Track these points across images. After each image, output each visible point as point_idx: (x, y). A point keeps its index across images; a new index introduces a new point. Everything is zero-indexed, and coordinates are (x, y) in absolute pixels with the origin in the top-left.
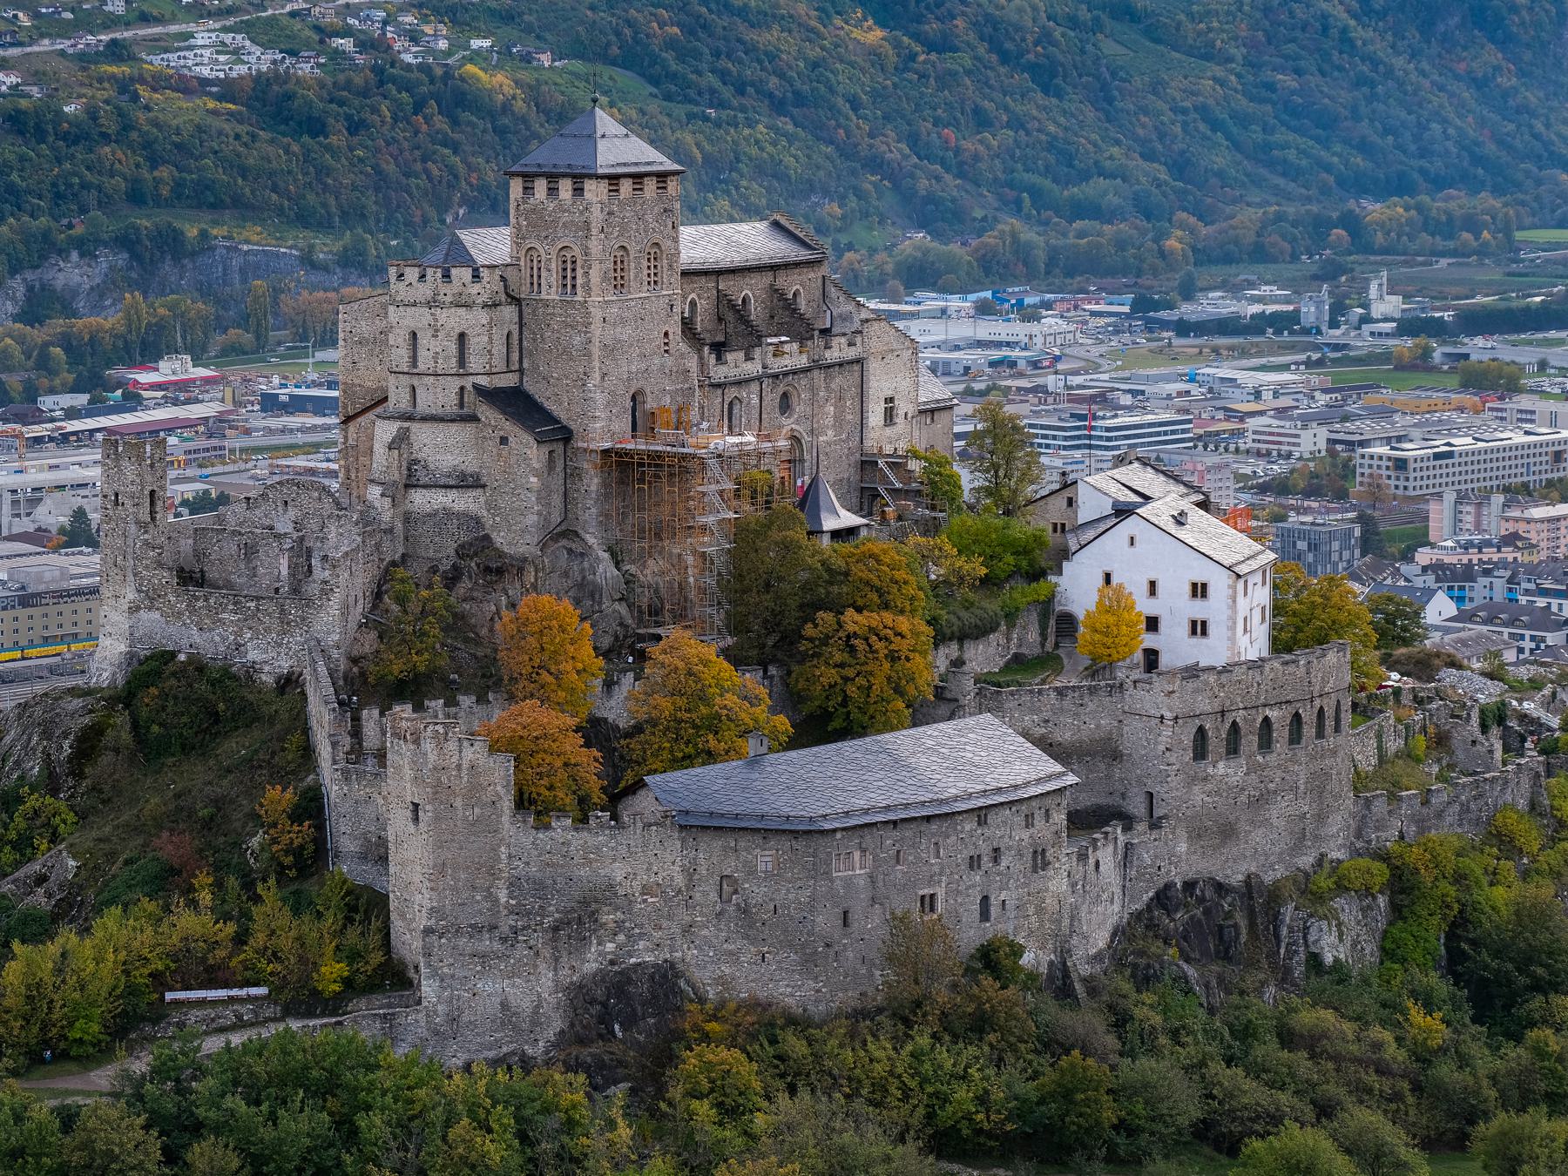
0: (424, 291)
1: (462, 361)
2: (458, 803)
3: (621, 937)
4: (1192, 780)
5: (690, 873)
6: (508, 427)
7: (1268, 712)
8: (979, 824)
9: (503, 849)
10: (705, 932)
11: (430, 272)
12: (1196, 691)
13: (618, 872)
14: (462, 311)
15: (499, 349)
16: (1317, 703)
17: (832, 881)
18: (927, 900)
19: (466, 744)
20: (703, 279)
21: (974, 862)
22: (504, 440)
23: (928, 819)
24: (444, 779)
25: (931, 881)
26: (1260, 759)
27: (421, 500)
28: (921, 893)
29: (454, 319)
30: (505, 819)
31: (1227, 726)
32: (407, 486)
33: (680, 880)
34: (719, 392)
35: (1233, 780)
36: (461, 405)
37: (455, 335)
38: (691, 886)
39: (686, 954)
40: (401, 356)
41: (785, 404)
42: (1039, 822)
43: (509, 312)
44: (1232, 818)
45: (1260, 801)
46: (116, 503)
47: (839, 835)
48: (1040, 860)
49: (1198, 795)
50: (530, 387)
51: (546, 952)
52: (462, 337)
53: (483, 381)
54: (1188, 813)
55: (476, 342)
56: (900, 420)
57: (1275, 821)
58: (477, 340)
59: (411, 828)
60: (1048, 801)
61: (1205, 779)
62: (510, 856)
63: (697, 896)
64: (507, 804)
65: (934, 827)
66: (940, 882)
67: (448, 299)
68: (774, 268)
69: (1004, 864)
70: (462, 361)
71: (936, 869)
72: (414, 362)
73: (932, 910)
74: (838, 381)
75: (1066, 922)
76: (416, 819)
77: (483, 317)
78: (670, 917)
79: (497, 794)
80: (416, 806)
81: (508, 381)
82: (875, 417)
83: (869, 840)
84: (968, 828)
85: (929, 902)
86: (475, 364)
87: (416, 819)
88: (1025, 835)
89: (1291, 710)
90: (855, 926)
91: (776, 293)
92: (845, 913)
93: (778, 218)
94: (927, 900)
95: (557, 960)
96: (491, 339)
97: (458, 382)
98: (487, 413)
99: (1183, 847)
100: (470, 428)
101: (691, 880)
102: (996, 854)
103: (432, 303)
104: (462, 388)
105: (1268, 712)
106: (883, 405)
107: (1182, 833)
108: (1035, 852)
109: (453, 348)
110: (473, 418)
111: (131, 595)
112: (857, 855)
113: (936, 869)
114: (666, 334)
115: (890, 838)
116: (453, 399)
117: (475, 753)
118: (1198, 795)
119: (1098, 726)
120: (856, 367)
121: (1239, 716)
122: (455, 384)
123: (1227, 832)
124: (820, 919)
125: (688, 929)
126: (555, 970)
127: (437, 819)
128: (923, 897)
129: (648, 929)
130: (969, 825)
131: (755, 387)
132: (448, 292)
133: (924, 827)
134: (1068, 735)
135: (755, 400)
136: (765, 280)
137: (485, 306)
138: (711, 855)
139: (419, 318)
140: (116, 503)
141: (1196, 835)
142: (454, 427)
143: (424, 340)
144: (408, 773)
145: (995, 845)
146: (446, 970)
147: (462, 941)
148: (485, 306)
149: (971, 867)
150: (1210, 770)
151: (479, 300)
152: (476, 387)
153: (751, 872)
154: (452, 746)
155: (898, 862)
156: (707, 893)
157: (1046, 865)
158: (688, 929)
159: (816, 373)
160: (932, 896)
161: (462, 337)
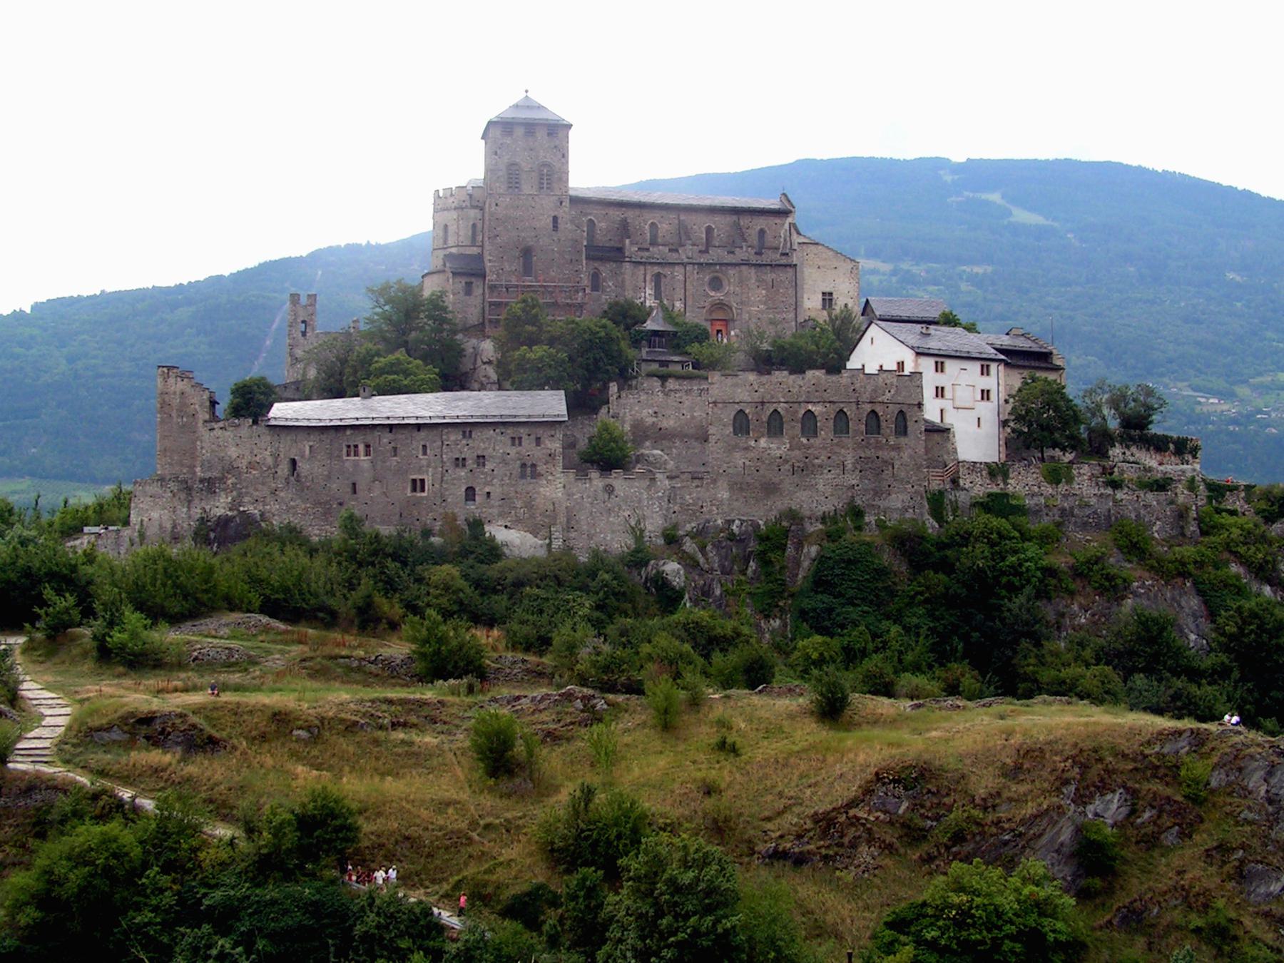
1: (445, 241)
2: (174, 414)
3: (235, 493)
4: (732, 449)
5: (276, 457)
7: (810, 407)
8: (464, 436)
9: (198, 443)
10: (282, 494)
12: (736, 385)
13: (233, 452)
16: (868, 408)
17: (343, 462)
18: (418, 483)
19: (179, 379)
20: (664, 213)
21: (460, 462)
23: (419, 427)
24: (167, 399)
25: (420, 470)
26: (804, 440)
28: (414, 477)
30: (200, 424)
31: (768, 413)
33: (270, 461)
34: (642, 268)
35: (778, 453)
36: (445, 265)
37: (442, 227)
38: (276, 465)
39: (273, 507)
41: (716, 284)
42: (528, 443)
43: (473, 213)
44: (776, 480)
45: (804, 470)
47: (348, 432)
48: (529, 470)
49: (739, 459)
51: (183, 496)
52: (446, 226)
53: (454, 250)
54: (730, 471)
55: (452, 229)
57: (821, 487)
60: (540, 432)
61: (747, 449)
62: (202, 448)
63: (279, 473)
65: (423, 434)
66: (427, 471)
69: (489, 466)
70: (445, 241)
71: (424, 463)
73: (423, 490)
74: (769, 276)
75: (562, 519)
77: (454, 215)
78: (263, 484)
79: (195, 409)
83: (371, 437)
85: (418, 485)
86: (450, 243)
88: (513, 451)
89: (837, 408)
90: (360, 494)
92: (354, 484)
94: (418, 483)
95: (190, 502)
96: (458, 228)
99: (726, 495)
101: (276, 461)
102: (481, 459)
105: (810, 407)
106: (820, 297)
107: (723, 483)
108: (524, 465)
109: (441, 233)
112: (361, 448)
113: (424, 463)
114: (555, 219)
115: (386, 437)
118: (739, 459)
119: (693, 417)
120: (790, 270)
121: (781, 408)
122: (441, 254)
123: (770, 489)
124: (334, 486)
125: (274, 492)
126: (189, 508)
128: (414, 481)
129: (251, 490)
130: (455, 436)
131: (677, 268)
133: (415, 433)
134: (672, 423)
135: (681, 277)
137: (455, 209)
138: (288, 448)
141: (738, 487)
145: (480, 453)
146: (141, 505)
147: (147, 488)
148: (455, 208)
149: (457, 466)
150: (752, 443)
151: (453, 206)
153: (303, 456)
154: (172, 380)
155: (395, 455)
156: (284, 469)
157: (536, 475)
158: (274, 492)
159: (744, 268)
160: (423, 481)
161: (446, 226)
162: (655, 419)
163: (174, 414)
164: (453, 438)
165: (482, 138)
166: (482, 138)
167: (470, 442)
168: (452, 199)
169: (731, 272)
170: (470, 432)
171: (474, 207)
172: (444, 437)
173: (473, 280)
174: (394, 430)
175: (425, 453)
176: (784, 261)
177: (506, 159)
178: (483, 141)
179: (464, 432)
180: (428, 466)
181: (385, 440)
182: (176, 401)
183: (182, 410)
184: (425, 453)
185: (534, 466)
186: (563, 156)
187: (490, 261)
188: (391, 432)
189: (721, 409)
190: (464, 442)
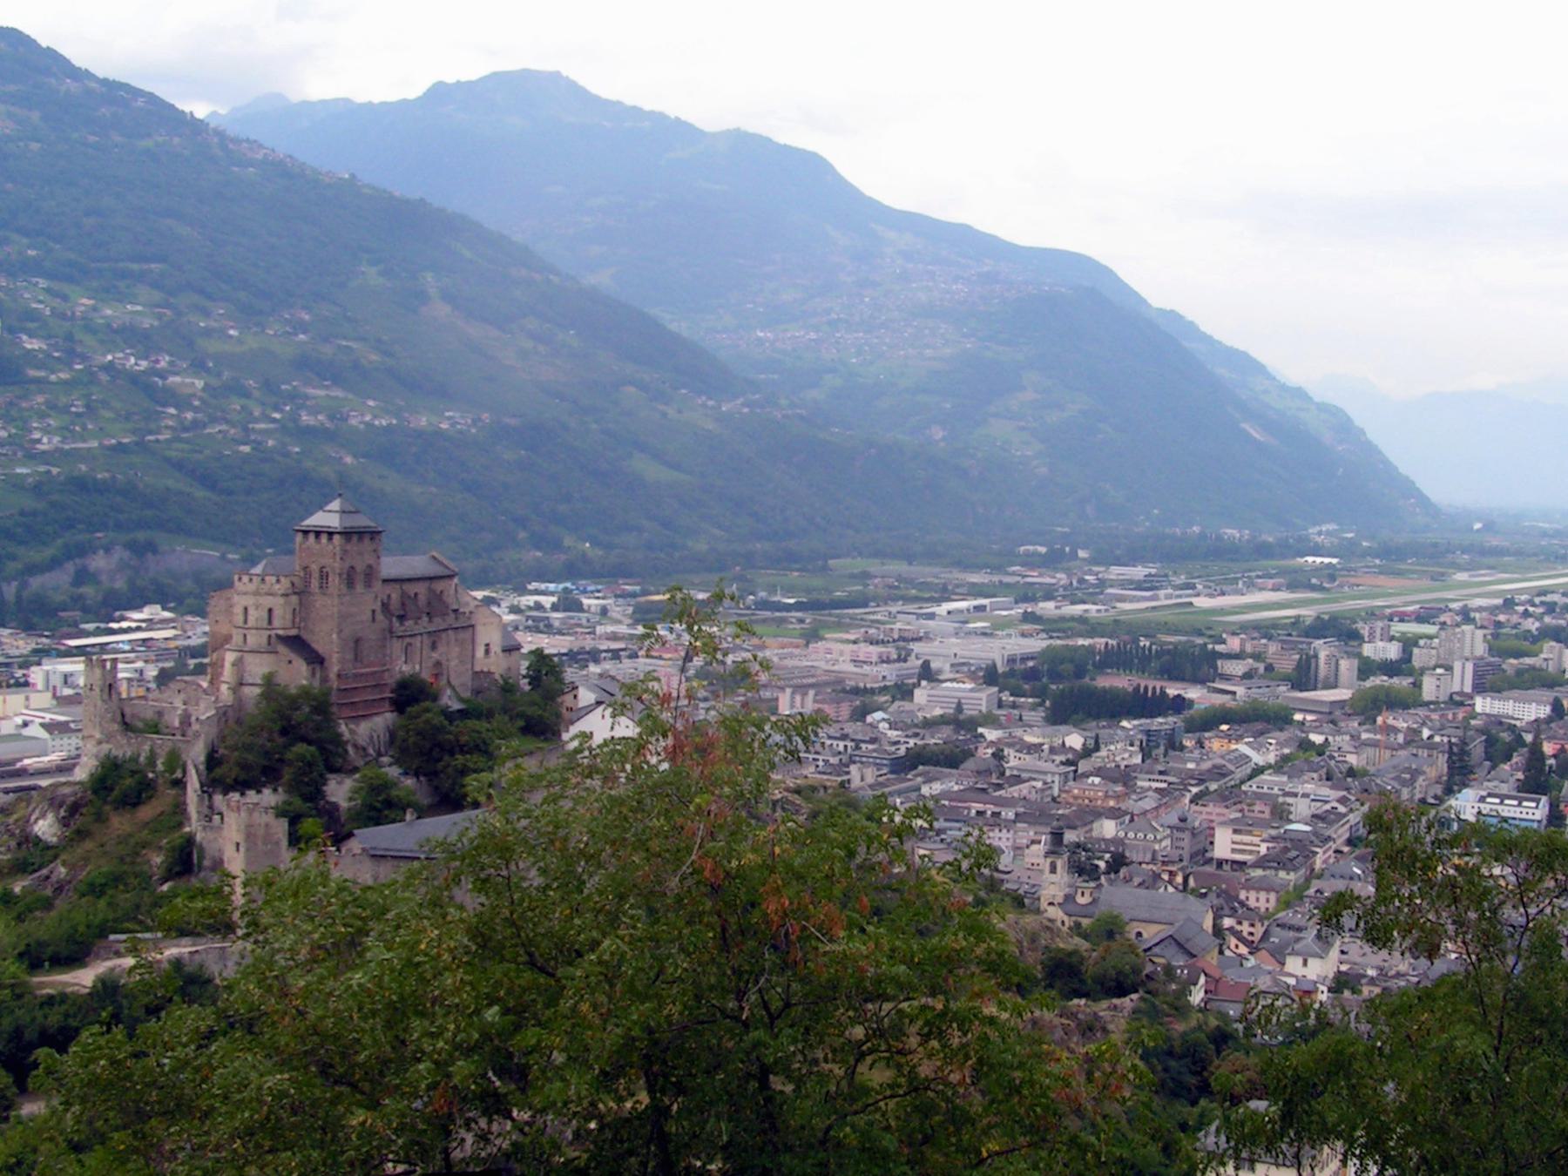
0: (251, 587)
1: (270, 622)
6: (292, 656)
11: (255, 578)
15: (289, 616)
22: (290, 662)
27: (247, 690)
29: (269, 602)
32: (241, 684)
36: (269, 644)
40: (239, 619)
41: (434, 647)
43: (294, 599)
46: (91, 689)
50: (305, 636)
52: (270, 610)
53: (281, 632)
55: (277, 613)
56: (492, 654)
59: (236, 854)
64: (285, 843)
68: (431, 579)
70: (270, 622)
72: (246, 622)
76: (238, 850)
77: (281, 600)
80: (238, 844)
81: (293, 632)
82: (480, 652)
86: (277, 623)
87: (238, 850)
91: (431, 590)
93: (435, 554)
97: (268, 632)
98: (282, 649)
100: (272, 656)
103: (256, 593)
104: (270, 636)
109: (265, 615)
110: (277, 652)
111: (98, 736)
116: (264, 640)
117: (269, 818)
127: (248, 850)
131: (419, 638)
132: (265, 588)
135: (419, 644)
136: (427, 584)
137: (283, 595)
139: (249, 601)
140: (91, 689)
142: (265, 656)
143: (251, 612)
144: (234, 827)
148: (283, 595)
151: (280, 592)
152: (278, 636)
161: (270, 610)
163: (260, 843)
168: (277, 586)
169: (444, 635)
171: (295, 593)
177: (347, 565)
182: (261, 831)
183: (268, 838)
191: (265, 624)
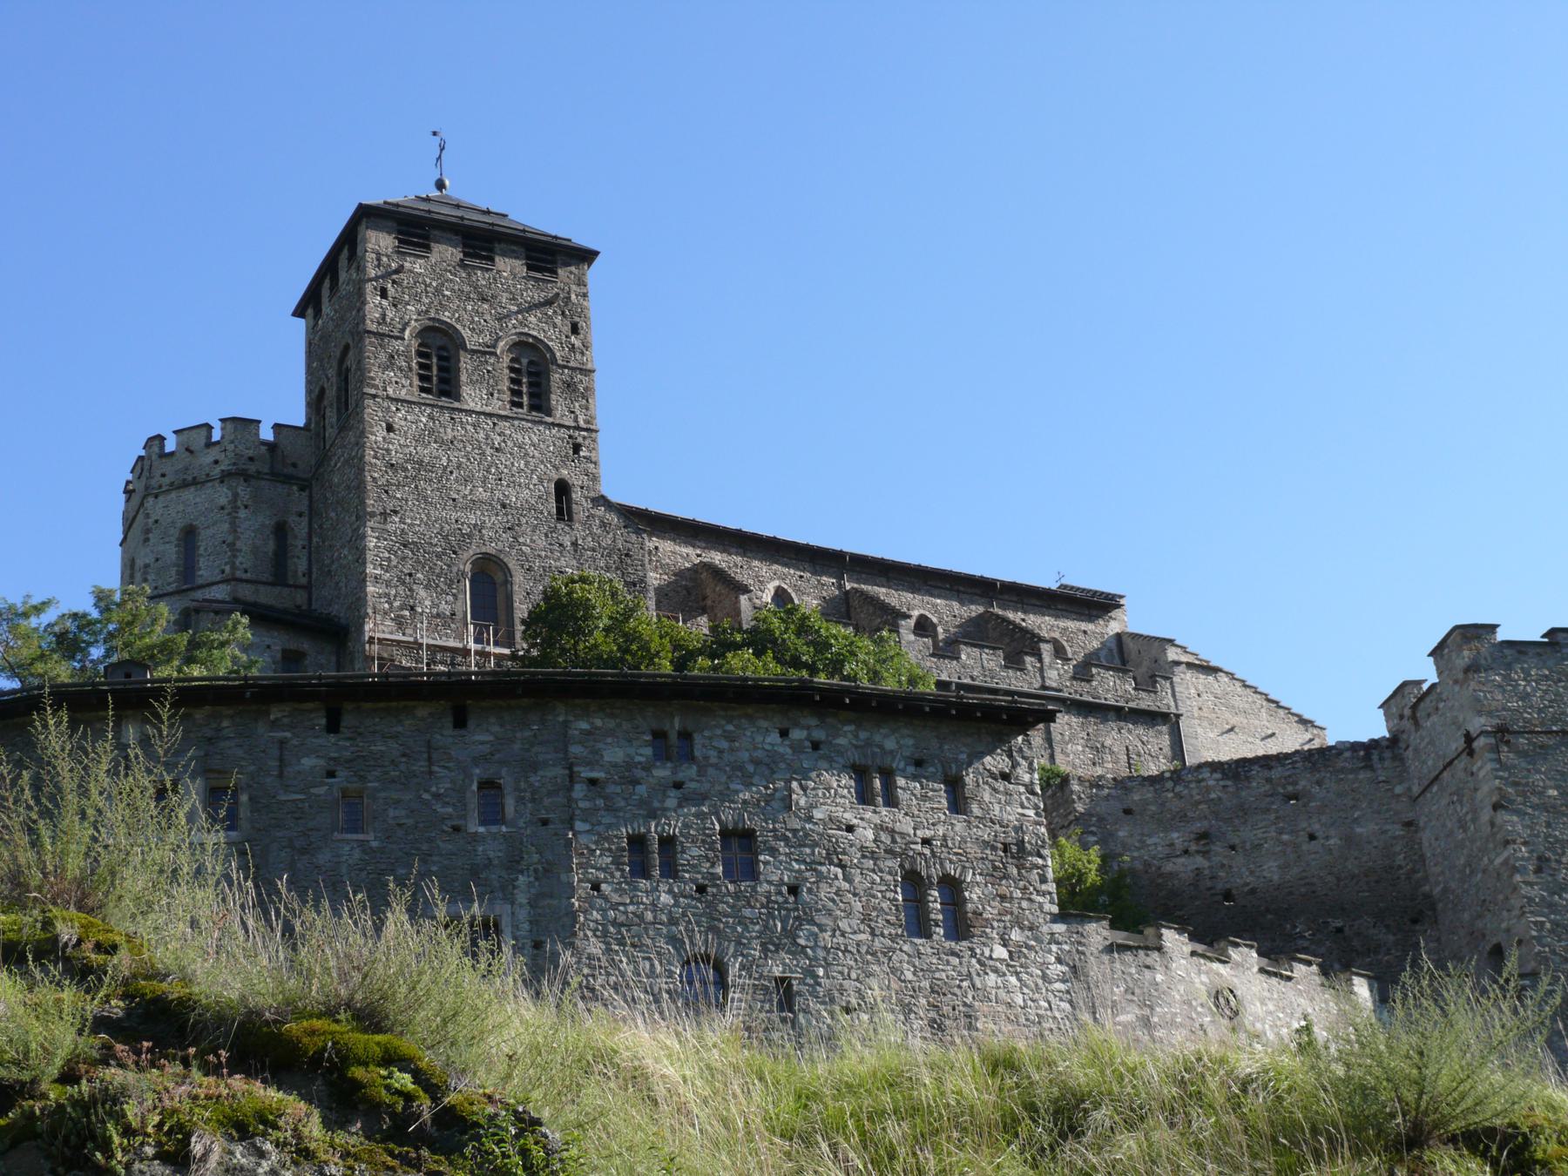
14: (189, 494)
37: (175, 533)
52: (189, 535)
58: (210, 532)
67: (166, 481)
84: (614, 754)
86: (205, 572)
96: (234, 529)
108: (913, 882)
109: (171, 552)
113: (492, 851)
119: (1349, 840)
137: (225, 477)
151: (217, 471)
155: (355, 826)
157: (961, 925)
162: (1200, 861)
164: (614, 754)
165: (299, 312)
166: (299, 312)
167: (688, 772)
170: (686, 736)
172: (576, 750)
173: (305, 645)
174: (348, 720)
175: (493, 814)
176: (1145, 702)
178: (301, 324)
179: (659, 735)
180: (514, 863)
181: (308, 762)
184: (493, 814)
185: (952, 887)
186: (575, 329)
187: (376, 578)
188: (333, 727)
189: (1523, 754)
190: (662, 772)
191: (171, 579)
